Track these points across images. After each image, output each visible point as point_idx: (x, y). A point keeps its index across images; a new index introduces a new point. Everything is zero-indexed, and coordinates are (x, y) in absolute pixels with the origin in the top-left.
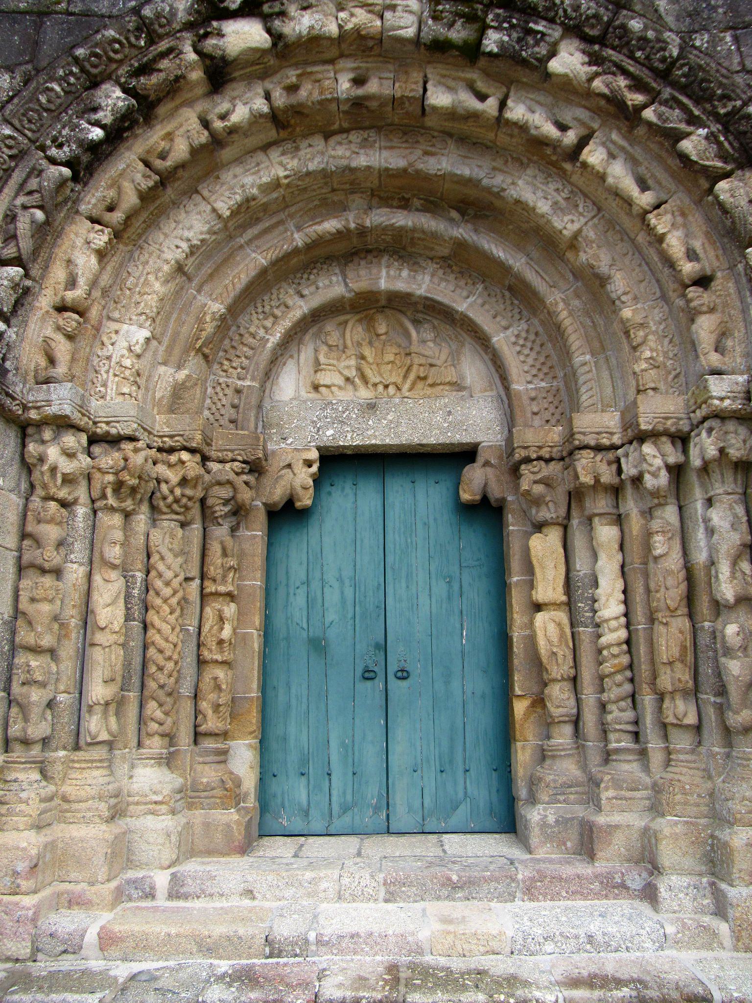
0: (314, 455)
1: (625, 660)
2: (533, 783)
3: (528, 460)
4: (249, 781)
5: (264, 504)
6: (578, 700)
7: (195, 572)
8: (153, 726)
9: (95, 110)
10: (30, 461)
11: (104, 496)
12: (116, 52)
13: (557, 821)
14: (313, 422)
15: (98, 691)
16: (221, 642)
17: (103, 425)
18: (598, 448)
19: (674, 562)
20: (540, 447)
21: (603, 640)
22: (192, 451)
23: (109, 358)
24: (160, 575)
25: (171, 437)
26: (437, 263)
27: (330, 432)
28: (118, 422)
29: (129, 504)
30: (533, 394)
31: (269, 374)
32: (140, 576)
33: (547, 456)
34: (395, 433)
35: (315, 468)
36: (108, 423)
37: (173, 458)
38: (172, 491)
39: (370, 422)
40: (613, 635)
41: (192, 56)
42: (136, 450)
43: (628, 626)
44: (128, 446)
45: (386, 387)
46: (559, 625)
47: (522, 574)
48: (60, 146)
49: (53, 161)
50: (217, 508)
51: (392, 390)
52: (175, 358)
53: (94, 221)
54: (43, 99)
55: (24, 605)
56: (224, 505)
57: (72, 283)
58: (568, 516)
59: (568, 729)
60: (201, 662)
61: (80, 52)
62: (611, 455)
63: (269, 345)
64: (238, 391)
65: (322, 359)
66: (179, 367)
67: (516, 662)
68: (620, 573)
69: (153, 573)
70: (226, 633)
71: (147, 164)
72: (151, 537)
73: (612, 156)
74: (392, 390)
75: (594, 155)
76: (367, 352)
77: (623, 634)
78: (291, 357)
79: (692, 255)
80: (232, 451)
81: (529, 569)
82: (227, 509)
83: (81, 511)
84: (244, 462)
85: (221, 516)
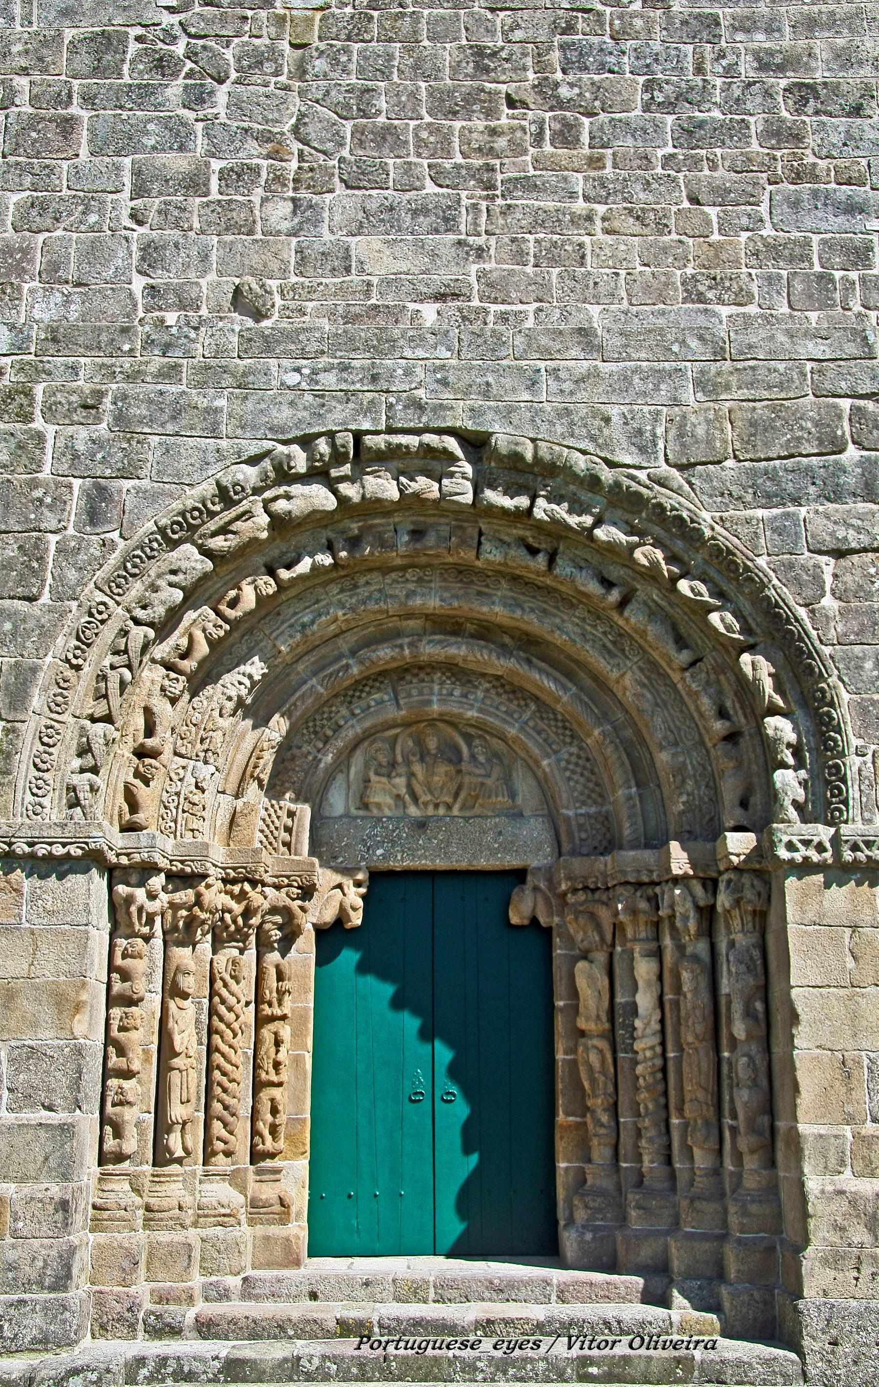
5: (314, 925)
6: (617, 1123)
7: (252, 997)
8: (220, 1146)
10: (117, 901)
12: (194, 518)
13: (594, 1238)
14: (364, 840)
17: (179, 864)
18: (639, 885)
20: (586, 878)
23: (178, 794)
25: (234, 869)
26: (490, 682)
27: (380, 852)
28: (193, 861)
30: (582, 820)
33: (592, 886)
34: (445, 853)
36: (182, 862)
37: (236, 889)
38: (234, 921)
39: (421, 842)
42: (208, 886)
45: (436, 806)
46: (601, 1051)
47: (569, 999)
50: (273, 933)
51: (441, 811)
55: (115, 1033)
56: (279, 929)
58: (613, 945)
62: (650, 892)
63: (322, 765)
65: (373, 777)
67: (560, 1086)
68: (657, 1002)
69: (217, 999)
72: (215, 964)
76: (418, 768)
78: (341, 771)
79: (722, 713)
80: (288, 877)
81: (574, 994)
84: (299, 887)
85: (275, 941)
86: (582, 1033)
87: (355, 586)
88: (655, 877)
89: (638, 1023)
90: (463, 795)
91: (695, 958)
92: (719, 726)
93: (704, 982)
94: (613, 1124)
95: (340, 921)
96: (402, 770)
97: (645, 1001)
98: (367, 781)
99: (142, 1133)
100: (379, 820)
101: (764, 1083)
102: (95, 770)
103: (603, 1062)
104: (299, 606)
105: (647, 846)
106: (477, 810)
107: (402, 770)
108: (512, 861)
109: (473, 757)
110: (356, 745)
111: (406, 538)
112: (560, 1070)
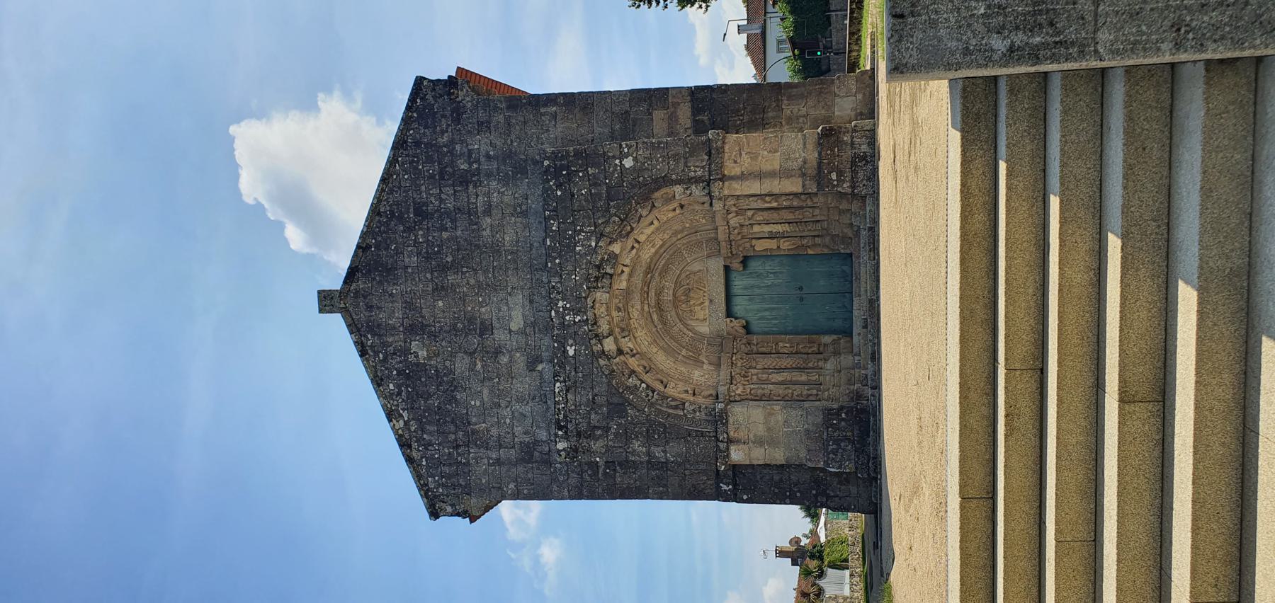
0: (728, 320)
1: (795, 224)
2: (834, 250)
3: (731, 252)
4: (835, 337)
9: (636, 385)
11: (748, 380)
15: (804, 378)
16: (791, 347)
18: (730, 233)
19: (765, 213)
21: (789, 231)
22: (732, 356)
24: (771, 364)
29: (750, 374)
30: (708, 249)
31: (700, 334)
32: (770, 371)
35: (733, 319)
40: (787, 228)
41: (617, 359)
43: (783, 223)
44: (733, 374)
45: (704, 296)
48: (648, 395)
49: (653, 397)
51: (705, 294)
52: (700, 364)
53: (666, 387)
54: (635, 400)
57: (687, 392)
59: (816, 239)
60: (796, 353)
61: (621, 391)
62: (731, 229)
64: (709, 344)
66: (703, 363)
70: (788, 345)
71: (647, 372)
73: (642, 233)
74: (705, 294)
75: (642, 238)
77: (787, 225)
79: (674, 210)
82: (749, 347)
83: (752, 386)
86: (779, 247)
87: (635, 328)
88: (727, 227)
89: (775, 231)
90: (701, 288)
91: (753, 215)
92: (678, 211)
93: (761, 213)
94: (808, 238)
95: (744, 327)
96: (692, 308)
97: (767, 228)
98: (697, 319)
99: (812, 389)
100: (710, 315)
101: (791, 197)
102: (700, 407)
103: (787, 241)
104: (643, 346)
105: (717, 229)
106: (705, 282)
107: (692, 308)
108: (722, 271)
109: (688, 284)
110: (685, 325)
111: (620, 313)
112: (792, 253)
